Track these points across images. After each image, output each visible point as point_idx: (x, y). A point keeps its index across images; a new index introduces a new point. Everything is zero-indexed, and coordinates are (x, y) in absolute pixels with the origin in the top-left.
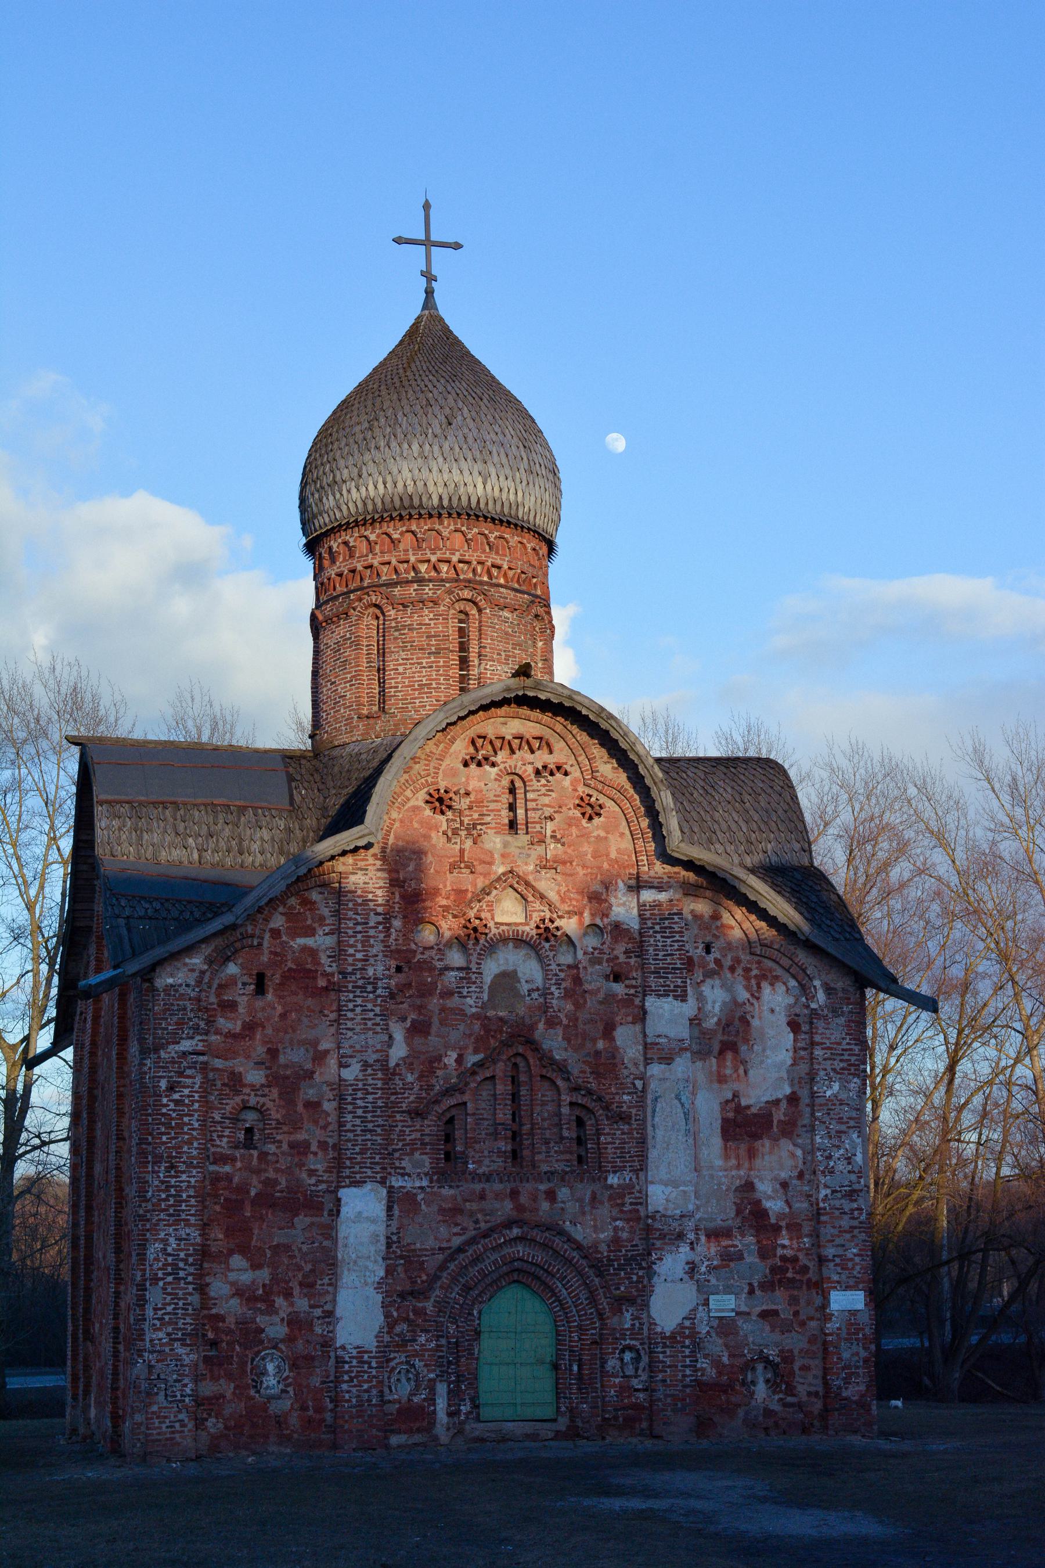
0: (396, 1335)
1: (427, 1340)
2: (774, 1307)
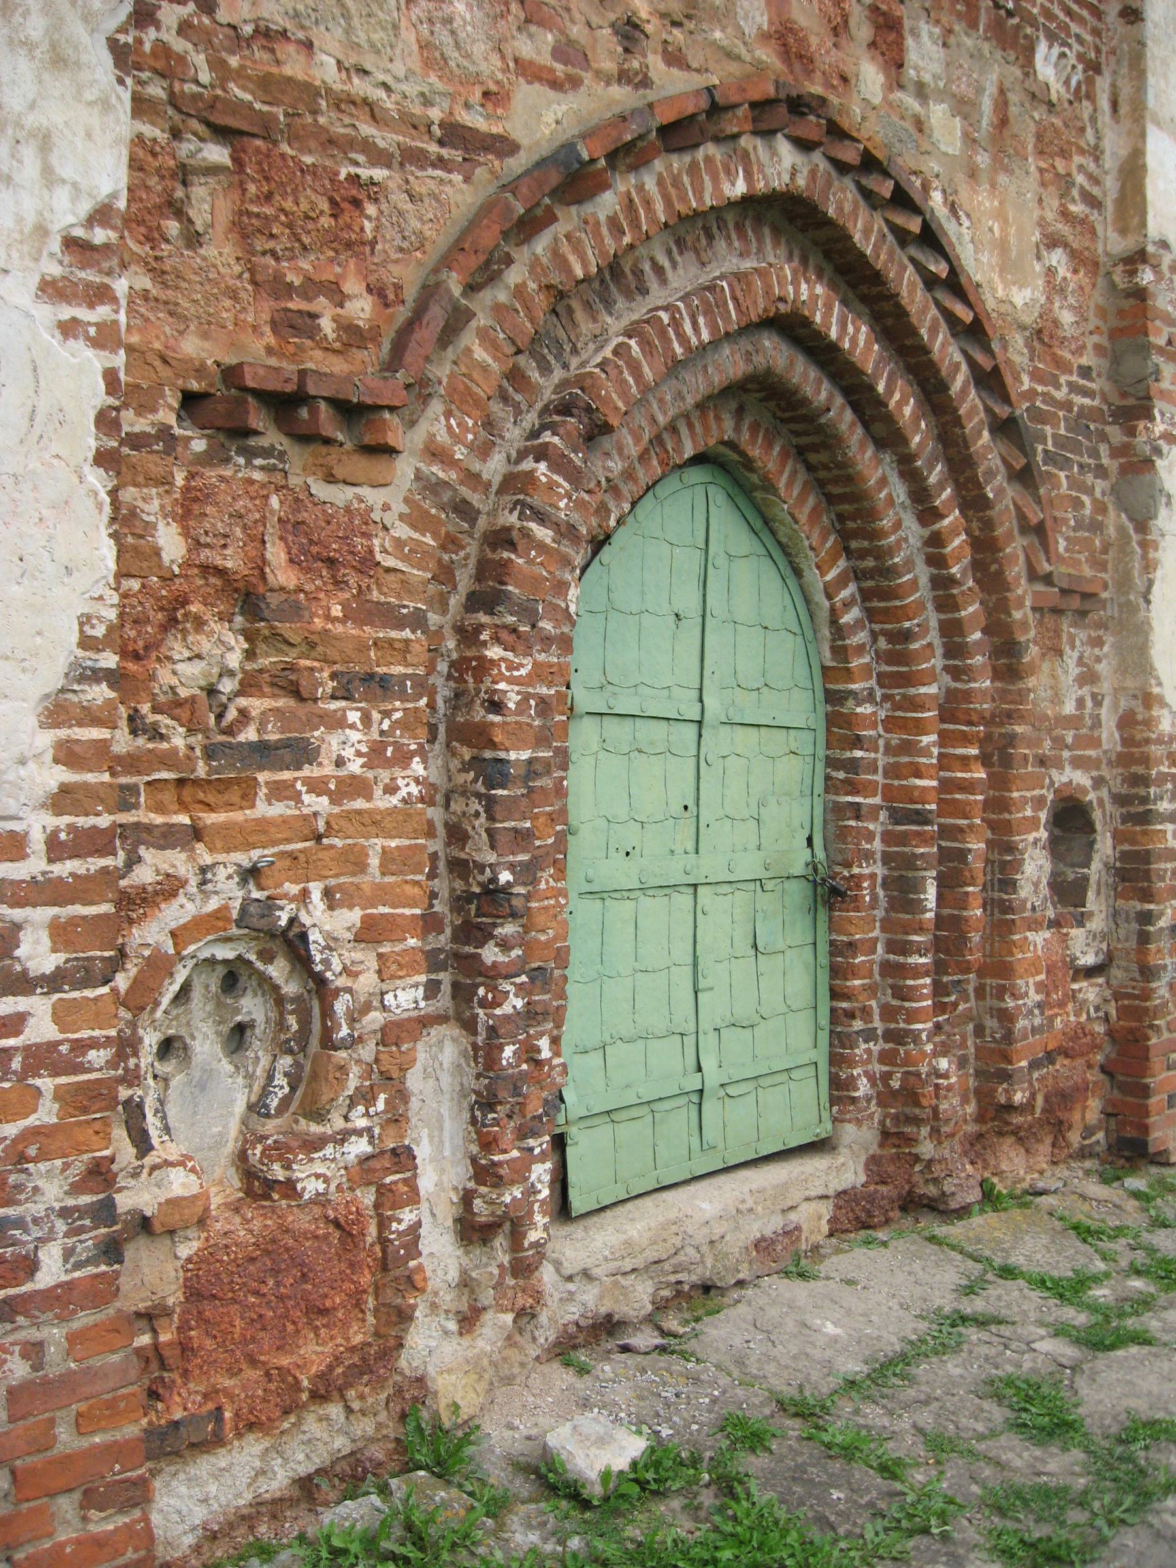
0: (174, 706)
1: (375, 755)
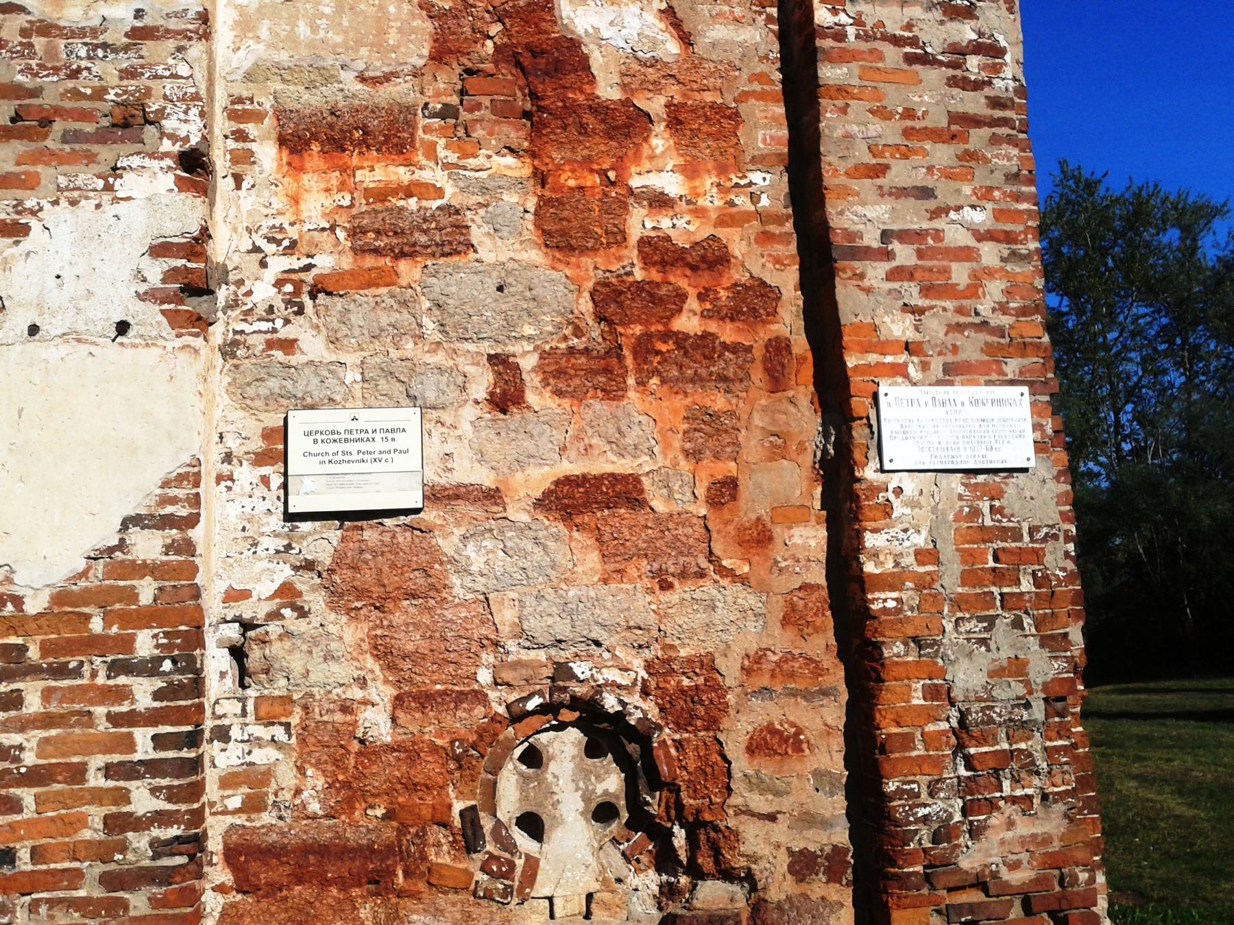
2: (623, 466)
